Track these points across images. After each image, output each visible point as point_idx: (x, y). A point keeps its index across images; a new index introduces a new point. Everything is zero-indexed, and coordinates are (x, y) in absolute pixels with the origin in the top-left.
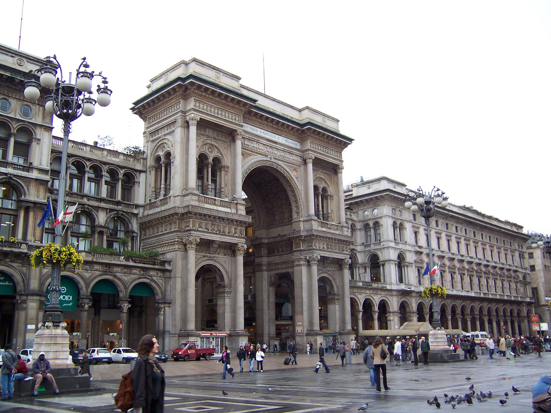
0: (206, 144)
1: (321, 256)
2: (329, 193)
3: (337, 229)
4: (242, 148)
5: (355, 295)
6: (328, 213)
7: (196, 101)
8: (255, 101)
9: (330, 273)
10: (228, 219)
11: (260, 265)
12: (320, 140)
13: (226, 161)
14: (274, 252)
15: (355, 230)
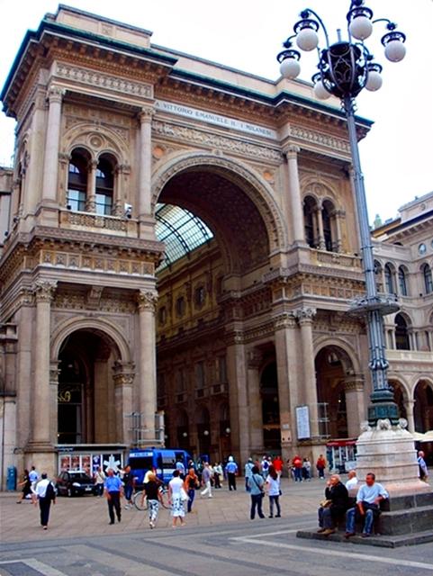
0: (87, 134)
1: (318, 310)
2: (337, 209)
3: (352, 265)
4: (152, 137)
5: (400, 376)
6: (338, 241)
7: (61, 67)
8: (174, 62)
9: (341, 337)
10: (116, 248)
11: (233, 334)
12: (309, 122)
13: (124, 159)
14: (251, 312)
15: (408, 275)
